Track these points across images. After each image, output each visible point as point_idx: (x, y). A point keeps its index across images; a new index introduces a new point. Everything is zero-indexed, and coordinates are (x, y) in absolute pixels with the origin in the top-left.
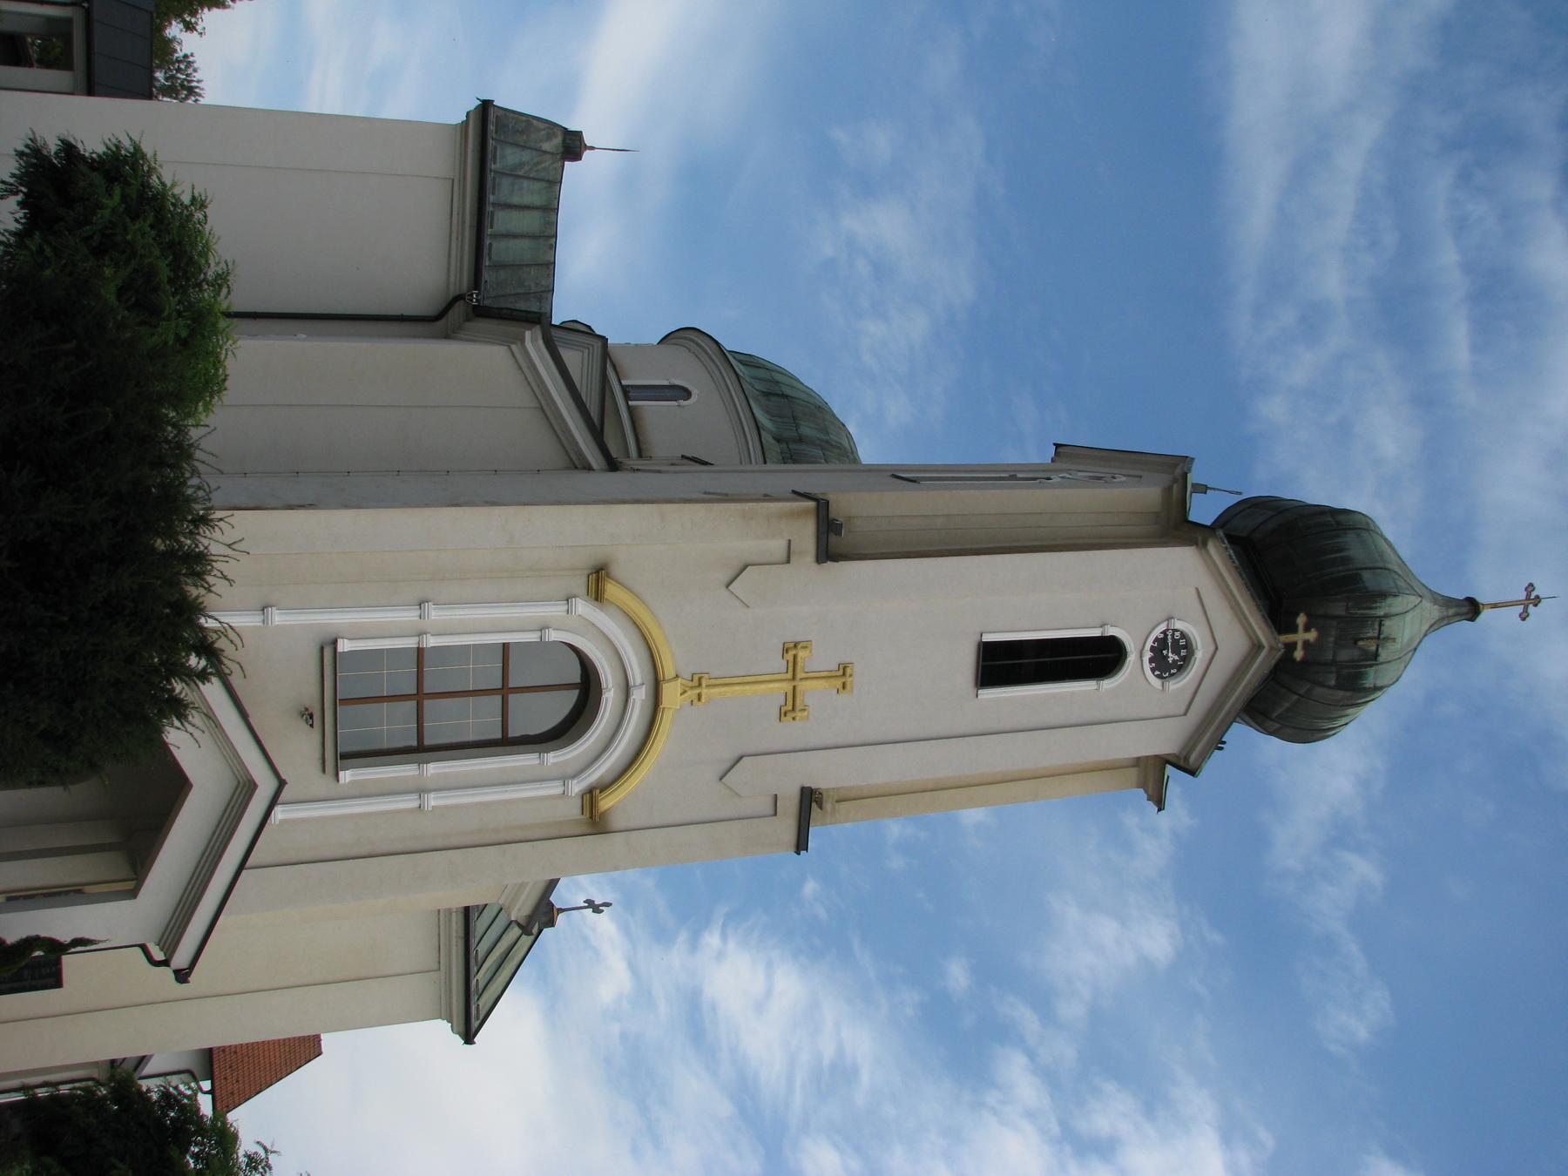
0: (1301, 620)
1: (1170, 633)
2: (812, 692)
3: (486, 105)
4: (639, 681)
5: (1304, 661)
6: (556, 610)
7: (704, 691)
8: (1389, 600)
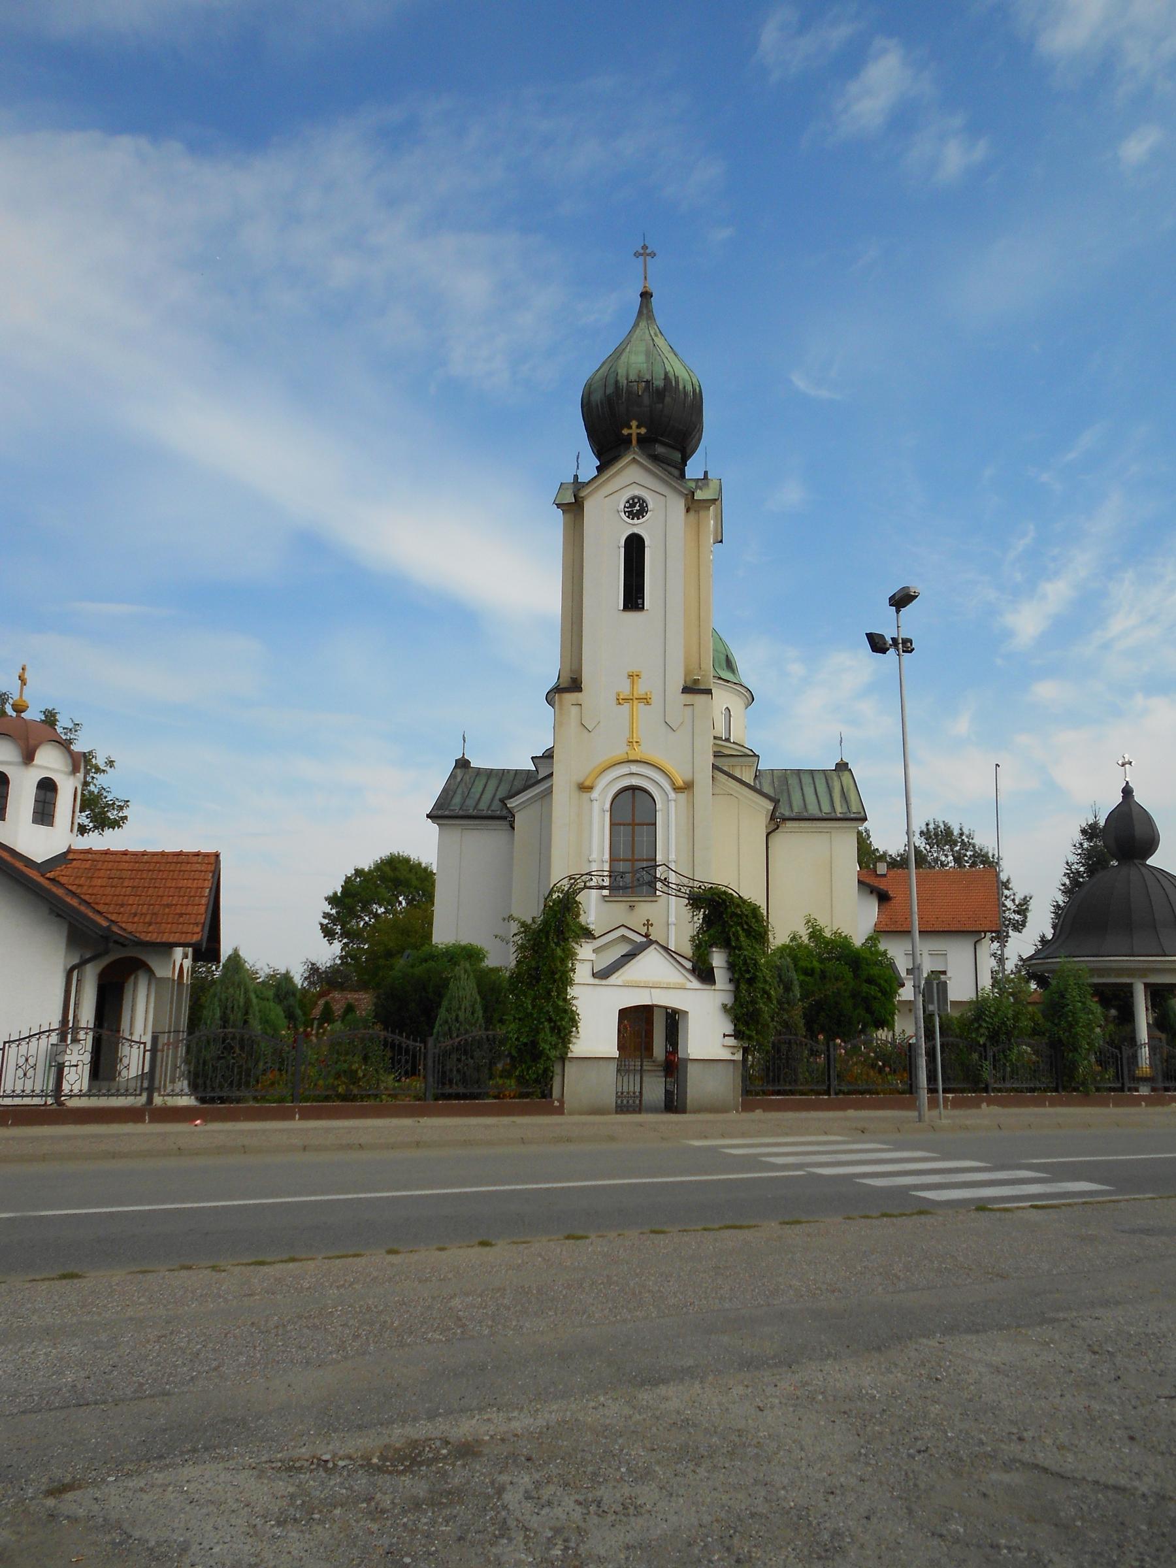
0: (625, 432)
1: (626, 510)
2: (641, 689)
3: (428, 816)
4: (628, 769)
5: (646, 427)
6: (596, 805)
7: (635, 740)
8: (619, 378)
